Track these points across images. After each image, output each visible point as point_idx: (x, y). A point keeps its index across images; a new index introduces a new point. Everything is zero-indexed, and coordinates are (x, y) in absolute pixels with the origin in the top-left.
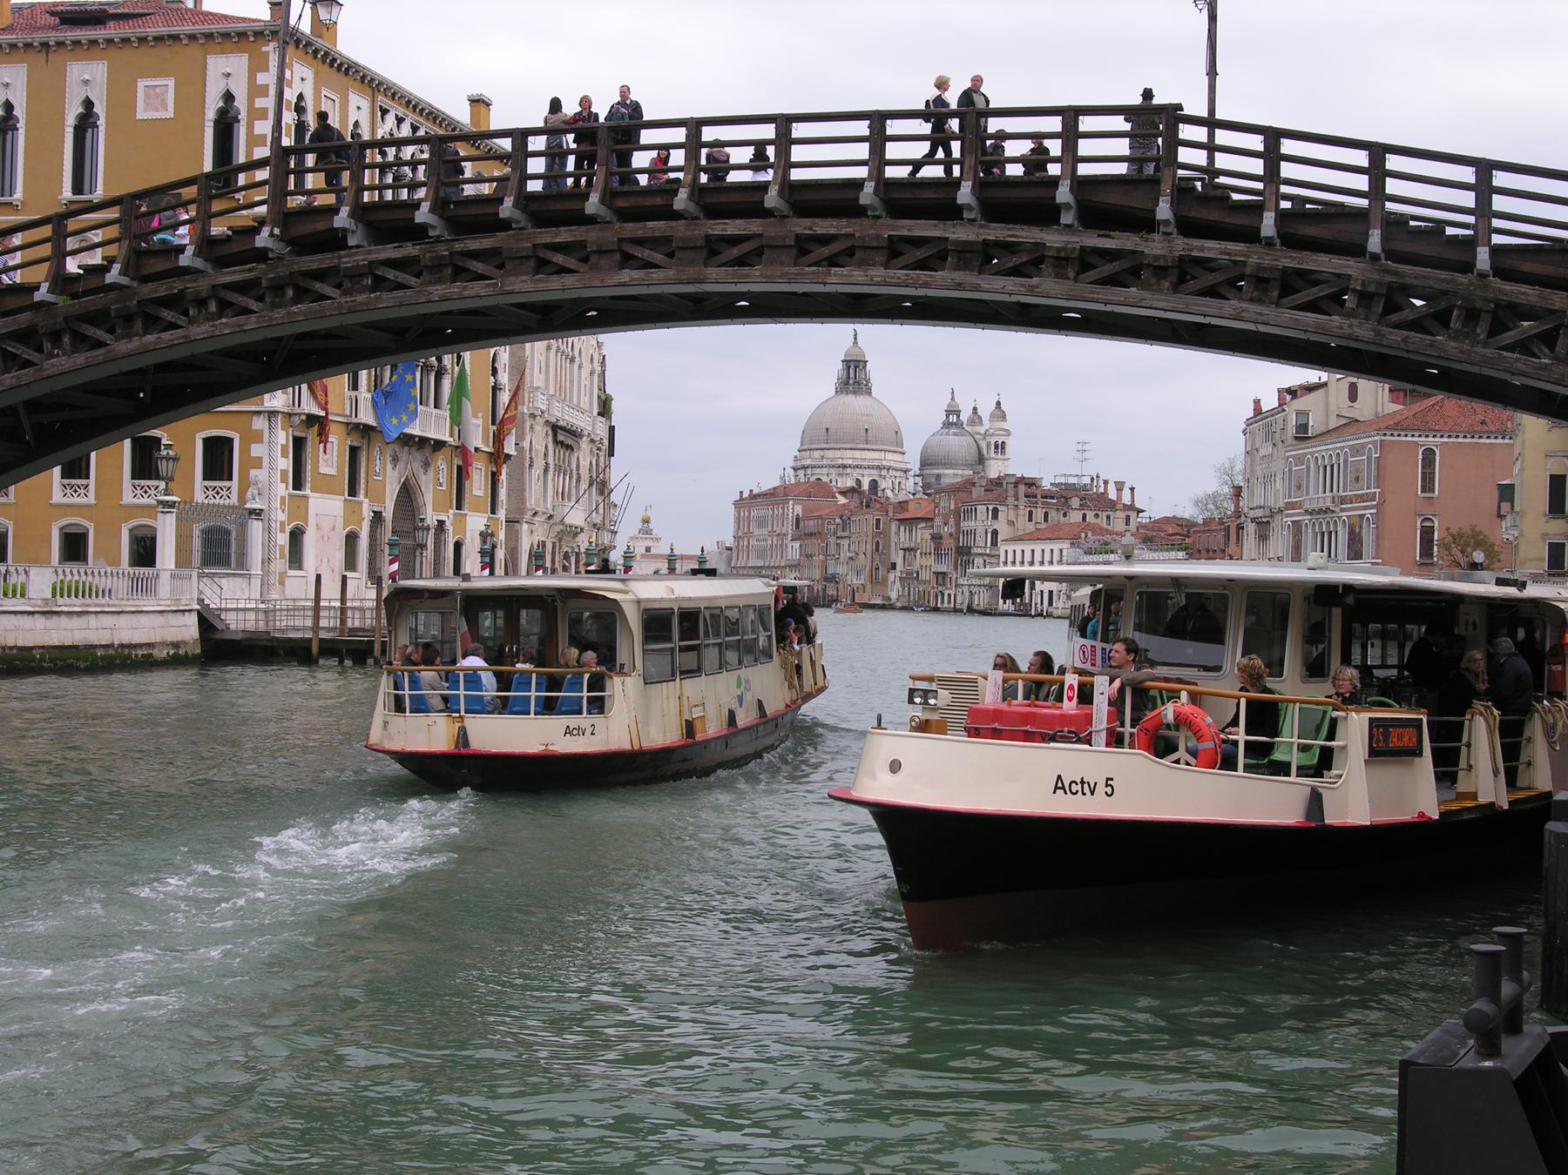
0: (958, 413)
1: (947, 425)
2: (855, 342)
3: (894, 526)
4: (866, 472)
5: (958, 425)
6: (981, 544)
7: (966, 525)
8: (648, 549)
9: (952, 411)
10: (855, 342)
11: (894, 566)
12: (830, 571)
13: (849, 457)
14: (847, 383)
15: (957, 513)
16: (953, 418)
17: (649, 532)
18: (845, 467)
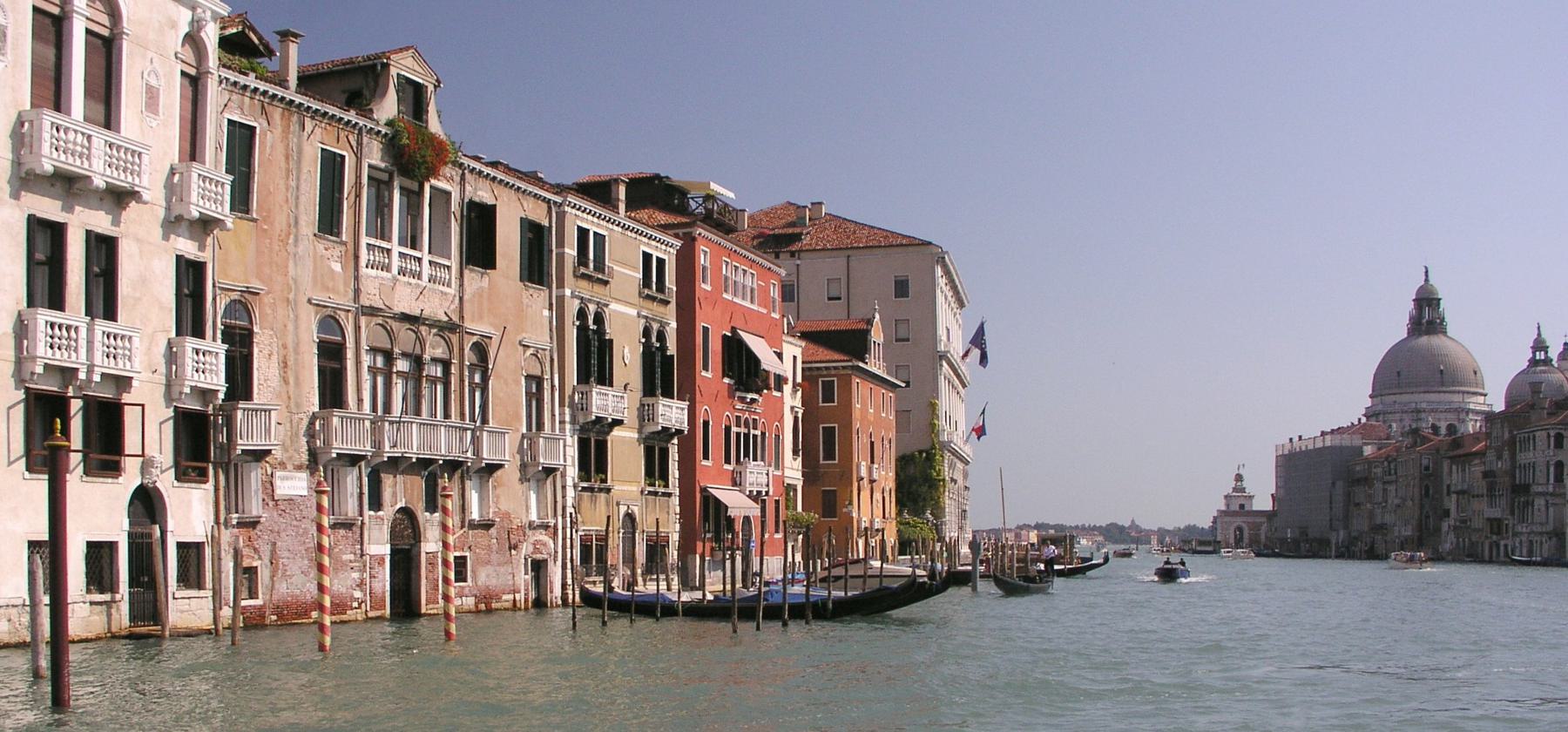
0: (1545, 349)
1: (1534, 362)
2: (1427, 280)
3: (1446, 464)
4: (1442, 416)
5: (1547, 362)
6: (1542, 482)
7: (1524, 458)
8: (1242, 506)
9: (1539, 345)
10: (1427, 280)
11: (1447, 513)
12: (1378, 521)
13: (1423, 400)
14: (1420, 324)
15: (1512, 443)
16: (1540, 356)
17: (1243, 490)
18: (1419, 411)
